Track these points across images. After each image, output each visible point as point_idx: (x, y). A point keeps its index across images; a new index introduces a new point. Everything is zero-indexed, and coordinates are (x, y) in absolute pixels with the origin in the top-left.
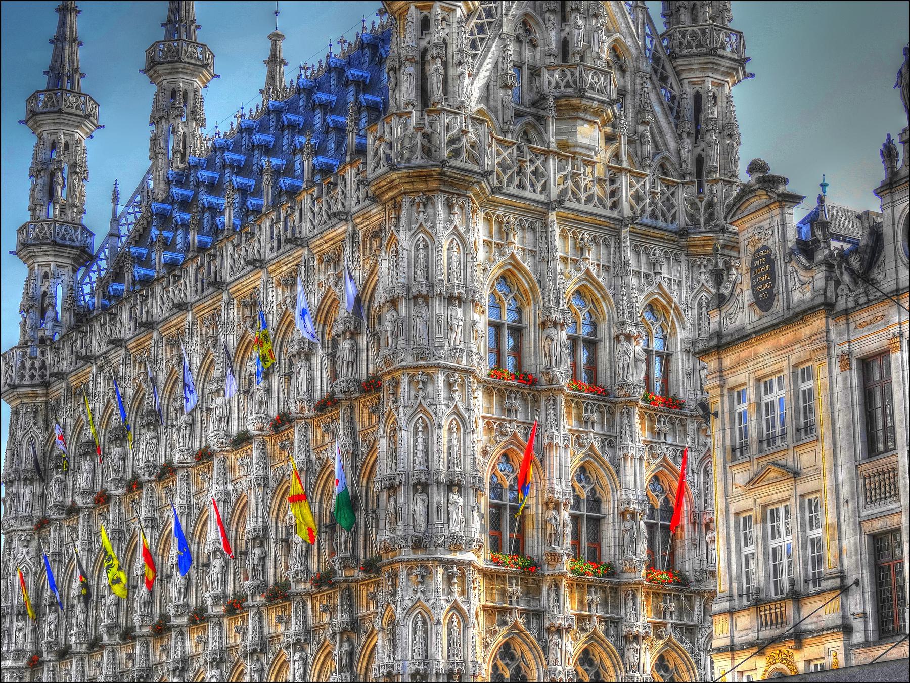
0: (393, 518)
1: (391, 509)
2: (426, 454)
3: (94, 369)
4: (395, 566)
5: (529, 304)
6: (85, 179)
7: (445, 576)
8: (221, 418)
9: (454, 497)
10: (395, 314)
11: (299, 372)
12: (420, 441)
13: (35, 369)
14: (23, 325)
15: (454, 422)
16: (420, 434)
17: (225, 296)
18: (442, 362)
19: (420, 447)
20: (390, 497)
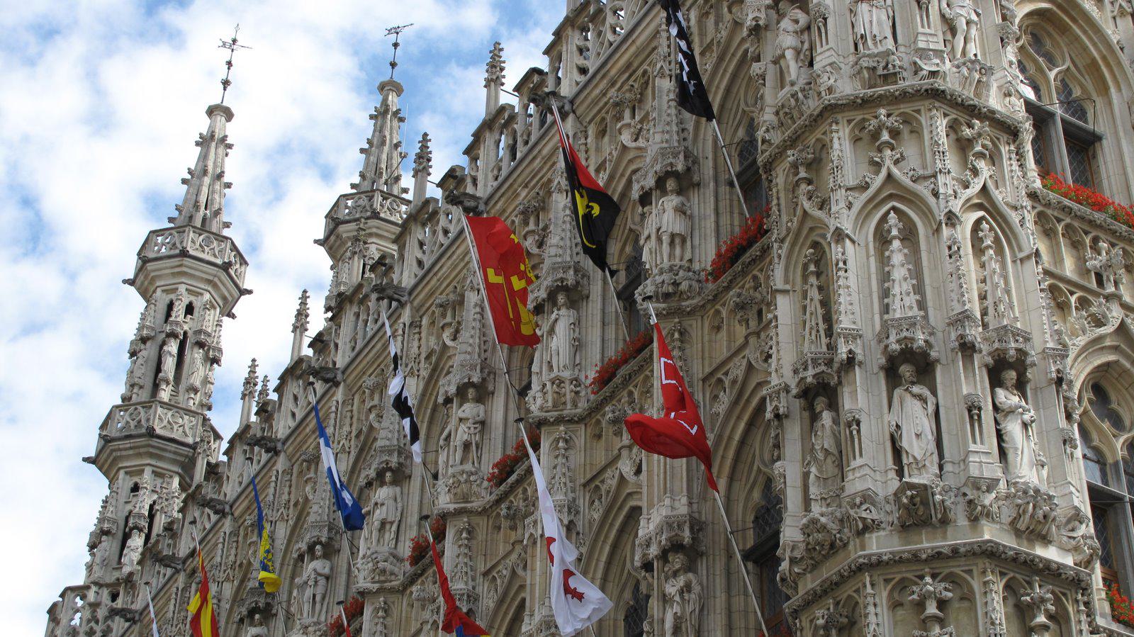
0: (830, 469)
1: (824, 439)
2: (919, 289)
3: (181, 579)
4: (847, 591)
5: (1104, 90)
6: (215, 361)
7: (1011, 609)
8: (383, 524)
9: (1008, 398)
10: (803, 18)
11: (552, 331)
12: (897, 258)
13: (97, 622)
14: (90, 567)
15: (985, 226)
16: (896, 244)
17: (406, 316)
18: (939, 84)
19: (899, 273)
20: (815, 417)
